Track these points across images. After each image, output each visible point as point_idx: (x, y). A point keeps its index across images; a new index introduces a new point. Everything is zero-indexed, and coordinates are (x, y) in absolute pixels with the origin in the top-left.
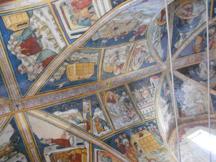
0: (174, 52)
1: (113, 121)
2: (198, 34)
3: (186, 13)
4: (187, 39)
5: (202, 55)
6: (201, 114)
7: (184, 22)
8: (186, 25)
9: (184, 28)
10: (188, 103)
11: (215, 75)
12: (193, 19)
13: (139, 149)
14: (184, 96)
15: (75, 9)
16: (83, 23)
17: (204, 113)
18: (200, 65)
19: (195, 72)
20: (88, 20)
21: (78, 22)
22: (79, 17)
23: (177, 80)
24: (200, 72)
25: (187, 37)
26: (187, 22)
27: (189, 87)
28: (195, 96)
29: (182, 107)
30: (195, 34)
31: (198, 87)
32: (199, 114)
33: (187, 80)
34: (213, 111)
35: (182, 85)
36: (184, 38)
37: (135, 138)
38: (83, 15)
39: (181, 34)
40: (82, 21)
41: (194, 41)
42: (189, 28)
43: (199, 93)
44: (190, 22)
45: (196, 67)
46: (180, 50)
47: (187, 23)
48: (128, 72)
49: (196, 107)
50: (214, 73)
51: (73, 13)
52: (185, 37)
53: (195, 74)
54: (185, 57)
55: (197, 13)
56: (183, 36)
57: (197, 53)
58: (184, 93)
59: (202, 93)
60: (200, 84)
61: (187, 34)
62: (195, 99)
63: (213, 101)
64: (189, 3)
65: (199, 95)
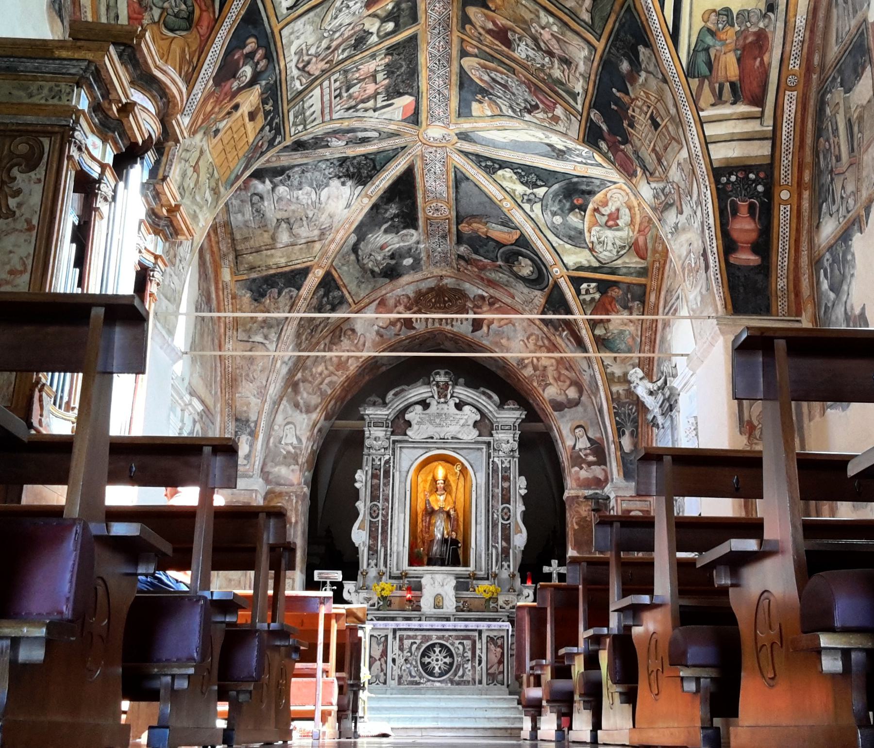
0: (483, 164)
1: (312, 14)
2: (526, 234)
3: (606, 211)
4: (519, 206)
5: (444, 237)
6: (233, 240)
7: (578, 201)
8: (568, 205)
9: (560, 201)
10: (280, 199)
12: (580, 226)
13: (221, 125)
14: (307, 189)
15: (745, 38)
16: (700, 49)
17: (235, 250)
18: (412, 231)
19: (392, 219)
20: (704, 69)
21: (709, 30)
22: (721, 40)
23: (374, 167)
24: (386, 231)
25: (527, 207)
26: (577, 210)
27: (343, 203)
28: (305, 223)
29: (264, 182)
30: (529, 230)
31: (338, 232)
32: (232, 234)
33: (366, 195)
34: (245, 277)
35: (349, 183)
36: (526, 197)
37: (250, 100)
38: (723, 58)
39: (541, 191)
40: (707, 50)
41: (507, 223)
42: (554, 214)
43: (316, 232)
44: (574, 219)
45: (409, 219)
46: (485, 183)
47: (572, 210)
48: (463, 40)
49: (264, 227)
50: (376, 269)
51: (737, 28)
52: (529, 201)
53: (384, 218)
54: (452, 191)
55: (594, 239)
56: (532, 197)
57: (458, 224)
58: (319, 187)
59: (315, 241)
60: (349, 236)
61: (537, 207)
62: (292, 221)
64: (632, 221)
65: (304, 232)
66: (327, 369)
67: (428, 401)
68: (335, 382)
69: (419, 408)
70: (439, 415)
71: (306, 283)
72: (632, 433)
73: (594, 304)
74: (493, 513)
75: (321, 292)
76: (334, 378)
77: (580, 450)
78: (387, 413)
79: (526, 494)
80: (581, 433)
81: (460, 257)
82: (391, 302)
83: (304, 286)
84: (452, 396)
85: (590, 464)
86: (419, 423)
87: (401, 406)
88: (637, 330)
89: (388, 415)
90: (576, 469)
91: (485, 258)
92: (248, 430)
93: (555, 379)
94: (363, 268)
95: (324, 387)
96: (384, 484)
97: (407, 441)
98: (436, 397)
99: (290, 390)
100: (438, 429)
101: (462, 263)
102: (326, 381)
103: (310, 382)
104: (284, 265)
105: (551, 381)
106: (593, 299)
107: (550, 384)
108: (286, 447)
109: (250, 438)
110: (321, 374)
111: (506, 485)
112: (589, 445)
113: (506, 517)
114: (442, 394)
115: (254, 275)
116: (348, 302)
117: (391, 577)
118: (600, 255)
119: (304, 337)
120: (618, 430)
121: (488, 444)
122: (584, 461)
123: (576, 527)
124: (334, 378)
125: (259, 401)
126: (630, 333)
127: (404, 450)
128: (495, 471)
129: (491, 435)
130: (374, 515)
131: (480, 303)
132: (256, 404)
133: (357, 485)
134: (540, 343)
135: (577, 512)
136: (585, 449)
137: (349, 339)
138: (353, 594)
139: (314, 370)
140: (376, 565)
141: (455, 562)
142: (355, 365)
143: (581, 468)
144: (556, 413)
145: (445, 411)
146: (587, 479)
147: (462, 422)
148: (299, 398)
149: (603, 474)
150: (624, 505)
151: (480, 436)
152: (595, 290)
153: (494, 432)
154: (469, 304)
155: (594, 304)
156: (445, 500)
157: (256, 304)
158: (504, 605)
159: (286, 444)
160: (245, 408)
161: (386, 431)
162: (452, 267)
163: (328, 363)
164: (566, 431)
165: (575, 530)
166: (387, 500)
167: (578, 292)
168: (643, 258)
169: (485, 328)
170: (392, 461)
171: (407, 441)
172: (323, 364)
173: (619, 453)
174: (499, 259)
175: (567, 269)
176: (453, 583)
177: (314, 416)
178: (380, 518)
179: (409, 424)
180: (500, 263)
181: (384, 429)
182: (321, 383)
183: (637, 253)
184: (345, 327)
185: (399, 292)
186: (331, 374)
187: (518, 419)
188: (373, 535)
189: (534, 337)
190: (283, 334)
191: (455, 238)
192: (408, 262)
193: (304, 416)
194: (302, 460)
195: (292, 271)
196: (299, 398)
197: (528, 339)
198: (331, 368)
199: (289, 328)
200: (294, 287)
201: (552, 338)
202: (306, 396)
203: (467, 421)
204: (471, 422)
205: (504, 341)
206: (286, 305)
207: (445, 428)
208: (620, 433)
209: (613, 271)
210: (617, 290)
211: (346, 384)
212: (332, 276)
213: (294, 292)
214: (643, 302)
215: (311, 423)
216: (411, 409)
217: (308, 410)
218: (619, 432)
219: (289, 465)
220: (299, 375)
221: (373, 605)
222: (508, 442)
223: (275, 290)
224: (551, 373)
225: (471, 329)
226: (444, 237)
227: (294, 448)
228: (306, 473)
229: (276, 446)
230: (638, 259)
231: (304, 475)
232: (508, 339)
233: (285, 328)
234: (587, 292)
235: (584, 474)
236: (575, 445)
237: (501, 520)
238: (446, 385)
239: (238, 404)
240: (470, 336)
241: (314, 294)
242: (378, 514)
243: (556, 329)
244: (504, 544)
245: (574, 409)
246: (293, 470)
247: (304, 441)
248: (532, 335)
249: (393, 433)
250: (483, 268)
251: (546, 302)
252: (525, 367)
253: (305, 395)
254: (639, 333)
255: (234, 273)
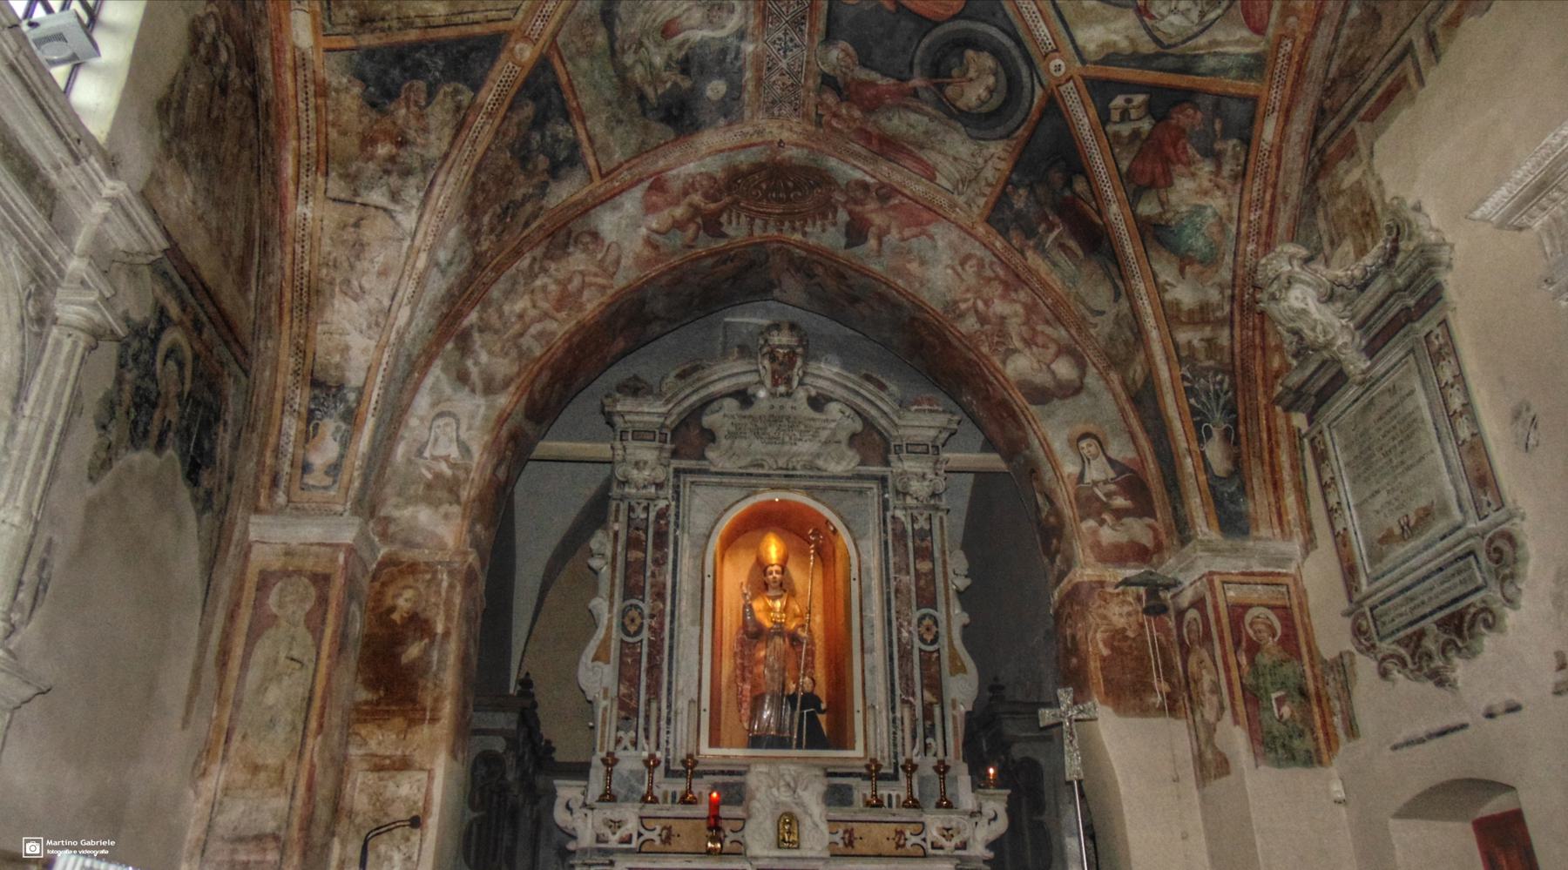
5: (797, 23)
11: (634, 96)
34: (349, 42)
50: (650, 91)
63: (440, 46)
66: (534, 306)
67: (750, 391)
68: (553, 334)
69: (731, 405)
70: (775, 419)
71: (493, 75)
72: (1226, 435)
73: (1138, 143)
74: (900, 626)
75: (528, 110)
76: (552, 326)
77: (1095, 483)
78: (663, 410)
79: (968, 588)
80: (1093, 449)
81: (828, 81)
82: (675, 186)
83: (489, 83)
84: (801, 383)
85: (1119, 514)
86: (732, 436)
87: (694, 398)
88: (1229, 205)
89: (667, 415)
90: (1091, 523)
91: (885, 75)
92: (341, 407)
93: (1024, 340)
94: (622, 73)
95: (526, 341)
96: (656, 562)
97: (705, 472)
98: (768, 382)
99: (450, 346)
100: (773, 448)
101: (830, 99)
102: (533, 330)
103: (496, 332)
104: (441, 21)
105: (1018, 344)
106: (1136, 134)
107: (1015, 351)
108: (434, 465)
109: (344, 426)
110: (521, 316)
111: (925, 566)
112: (1112, 474)
113: (929, 637)
114: (781, 376)
115: (368, 40)
116: (585, 166)
117: (669, 773)
118: (1161, 25)
119: (486, 219)
120: (1198, 425)
121: (883, 480)
122: (1106, 507)
123: (1105, 652)
124: (552, 326)
125: (373, 343)
126: (1215, 214)
127: (698, 490)
128: (900, 536)
129: (887, 463)
130: (632, 629)
131: (859, 194)
132: (365, 351)
133: (595, 563)
134: (988, 273)
135: (1105, 617)
136: (1106, 482)
137: (585, 250)
138: (579, 813)
139: (506, 308)
140: (635, 744)
141: (815, 739)
142: (596, 303)
143: (1102, 522)
144: (1033, 408)
145: (788, 411)
146: (1117, 547)
147: (824, 434)
148: (470, 363)
149: (1151, 534)
150: (1231, 594)
151: (862, 463)
152: (1142, 112)
153: (892, 457)
154: (839, 197)
155: (1138, 143)
156: (785, 609)
157: (374, 115)
158: (943, 841)
159: (435, 458)
160: (337, 358)
161: (661, 449)
162: (806, 115)
163: (539, 296)
164: (1059, 445)
165: (1103, 659)
166: (660, 596)
167: (1104, 117)
168: (1259, 30)
169: (872, 243)
170: (672, 512)
171: (705, 472)
172: (526, 297)
173: (1203, 478)
174: (917, 70)
175: (1084, 62)
176: (820, 786)
177: (503, 400)
178: (645, 635)
179: (710, 436)
180: (917, 82)
181: (656, 444)
182: (521, 335)
183: (1247, 17)
184: (577, 226)
185: (691, 167)
186: (546, 315)
187: (942, 429)
188: (626, 675)
189: (973, 262)
190: (436, 190)
191: (821, 25)
192: (716, 89)
193: (480, 401)
194: (466, 493)
195: (461, 40)
196: (470, 363)
197: (962, 264)
198: (545, 305)
199: (451, 180)
200: (466, 81)
201: (1016, 259)
202: (485, 358)
203: (834, 433)
204: (843, 436)
205: (914, 267)
206: (444, 124)
207: (786, 448)
208: (1202, 435)
209: (1187, 65)
210: (1190, 111)
211: (575, 340)
212: (554, 73)
213: (466, 97)
214: (1247, 141)
215: (494, 415)
216: (715, 405)
217: (489, 388)
218: (1198, 429)
219: (434, 503)
220: (473, 317)
221: (628, 840)
222: (923, 476)
223: (421, 85)
224: (1015, 327)
225: (843, 242)
226: (797, 23)
227: (453, 466)
228: (478, 527)
229: (409, 462)
230: (1245, 33)
231: (471, 531)
232: (923, 263)
233: (440, 179)
234: (1125, 116)
235: (1108, 535)
236: (1081, 476)
237: (917, 643)
238: (792, 356)
239: (320, 351)
240: (841, 253)
241: (511, 108)
242: (641, 626)
243: (1029, 232)
244: (928, 696)
245: (1069, 401)
246: (446, 516)
247: (476, 450)
248: (968, 257)
249: (675, 454)
250: (872, 106)
251: (1014, 169)
252: (961, 316)
253: (484, 357)
254: (1235, 214)
255: (320, 30)
